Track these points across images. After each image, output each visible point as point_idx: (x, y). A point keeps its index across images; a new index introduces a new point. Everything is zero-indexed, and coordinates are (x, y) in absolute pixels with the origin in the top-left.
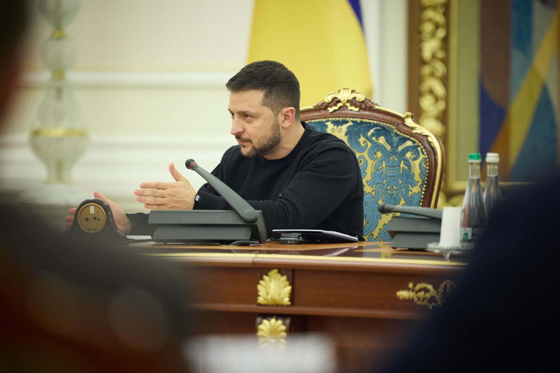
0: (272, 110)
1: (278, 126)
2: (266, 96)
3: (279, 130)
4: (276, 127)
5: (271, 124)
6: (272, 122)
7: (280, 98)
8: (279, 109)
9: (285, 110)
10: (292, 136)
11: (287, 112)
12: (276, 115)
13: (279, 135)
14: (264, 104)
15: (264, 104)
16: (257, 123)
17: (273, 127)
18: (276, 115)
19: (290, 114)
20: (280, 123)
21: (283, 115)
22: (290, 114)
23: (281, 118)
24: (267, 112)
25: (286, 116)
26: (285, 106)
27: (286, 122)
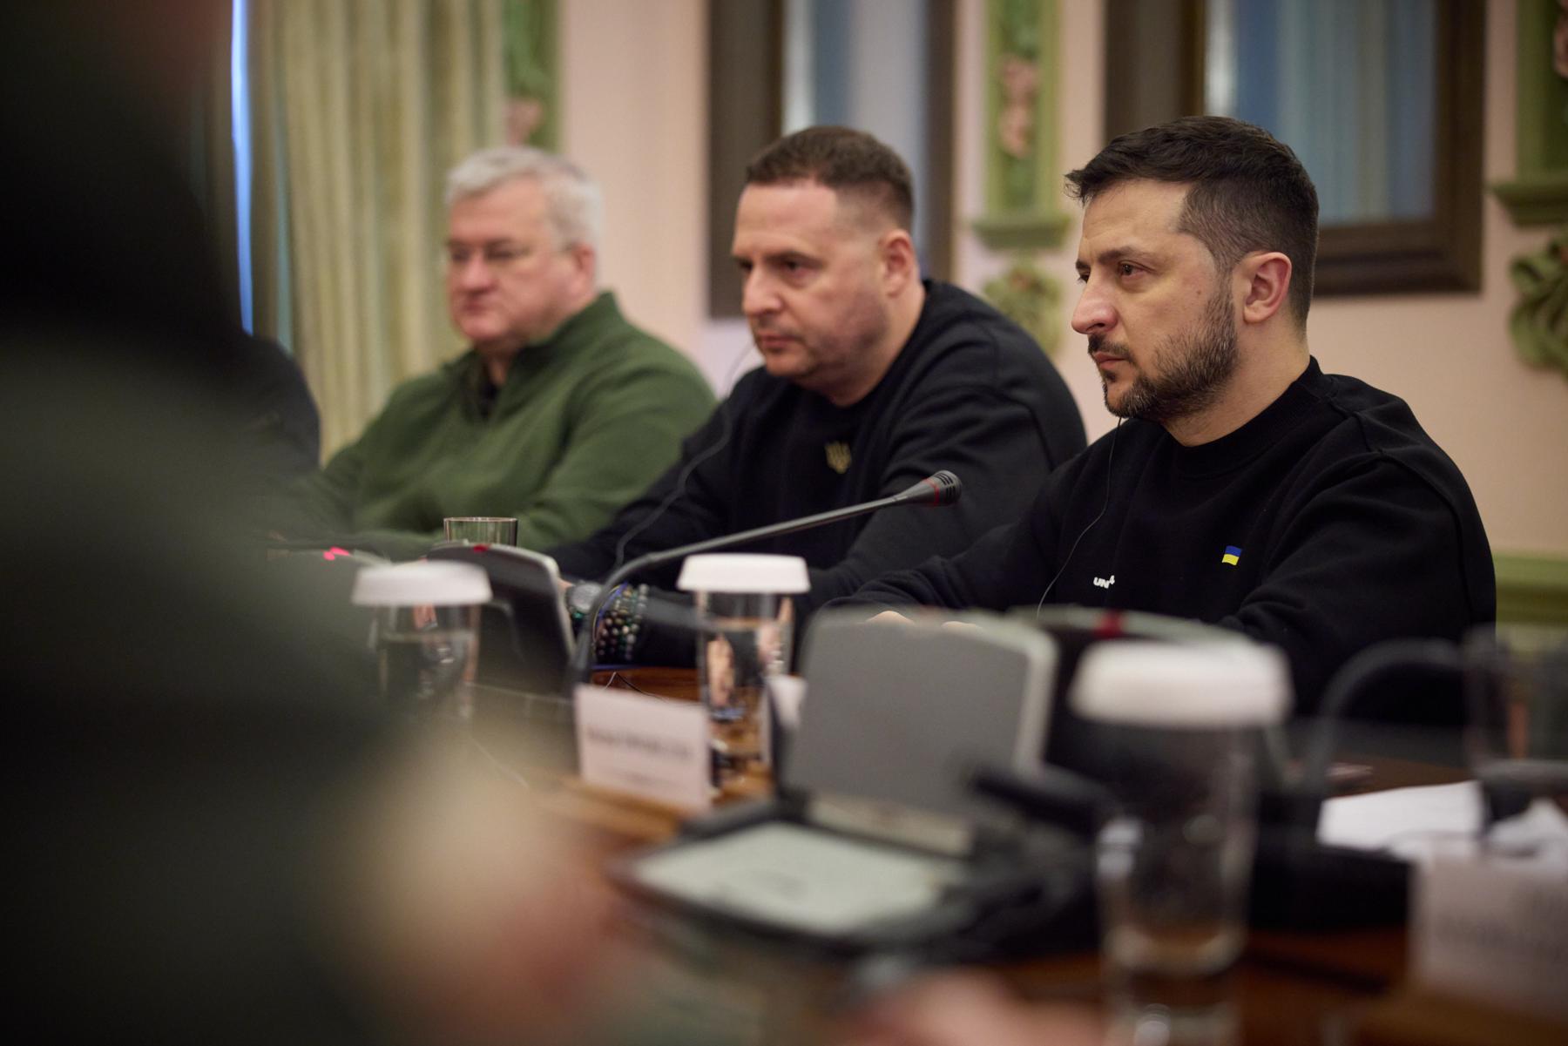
0: (1212, 251)
1: (1229, 310)
2: (1192, 201)
3: (1230, 323)
4: (1220, 312)
5: (1205, 297)
6: (1209, 288)
7: (1241, 218)
8: (1236, 250)
9: (1256, 259)
11: (1264, 266)
12: (1226, 271)
13: (1232, 342)
14: (1184, 228)
15: (1184, 228)
16: (1158, 291)
17: (1209, 308)
19: (1272, 275)
21: (1246, 275)
22: (1272, 275)
23: (1241, 287)
24: (1195, 255)
26: (1257, 246)
27: (1257, 303)
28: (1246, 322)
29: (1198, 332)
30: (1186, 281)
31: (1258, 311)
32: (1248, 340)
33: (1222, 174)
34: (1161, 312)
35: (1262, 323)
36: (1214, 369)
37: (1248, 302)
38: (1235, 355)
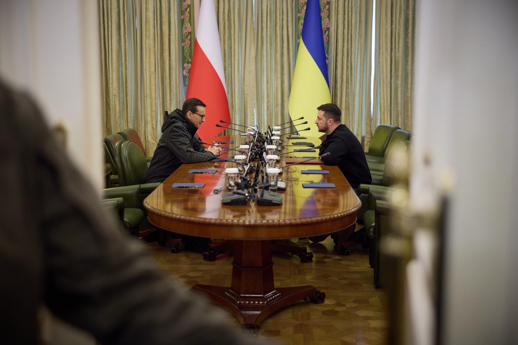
2: (325, 113)
4: (326, 124)
12: (327, 120)
16: (321, 121)
18: (327, 120)
23: (328, 122)
24: (324, 118)
31: (330, 124)
32: (329, 127)
34: (321, 123)
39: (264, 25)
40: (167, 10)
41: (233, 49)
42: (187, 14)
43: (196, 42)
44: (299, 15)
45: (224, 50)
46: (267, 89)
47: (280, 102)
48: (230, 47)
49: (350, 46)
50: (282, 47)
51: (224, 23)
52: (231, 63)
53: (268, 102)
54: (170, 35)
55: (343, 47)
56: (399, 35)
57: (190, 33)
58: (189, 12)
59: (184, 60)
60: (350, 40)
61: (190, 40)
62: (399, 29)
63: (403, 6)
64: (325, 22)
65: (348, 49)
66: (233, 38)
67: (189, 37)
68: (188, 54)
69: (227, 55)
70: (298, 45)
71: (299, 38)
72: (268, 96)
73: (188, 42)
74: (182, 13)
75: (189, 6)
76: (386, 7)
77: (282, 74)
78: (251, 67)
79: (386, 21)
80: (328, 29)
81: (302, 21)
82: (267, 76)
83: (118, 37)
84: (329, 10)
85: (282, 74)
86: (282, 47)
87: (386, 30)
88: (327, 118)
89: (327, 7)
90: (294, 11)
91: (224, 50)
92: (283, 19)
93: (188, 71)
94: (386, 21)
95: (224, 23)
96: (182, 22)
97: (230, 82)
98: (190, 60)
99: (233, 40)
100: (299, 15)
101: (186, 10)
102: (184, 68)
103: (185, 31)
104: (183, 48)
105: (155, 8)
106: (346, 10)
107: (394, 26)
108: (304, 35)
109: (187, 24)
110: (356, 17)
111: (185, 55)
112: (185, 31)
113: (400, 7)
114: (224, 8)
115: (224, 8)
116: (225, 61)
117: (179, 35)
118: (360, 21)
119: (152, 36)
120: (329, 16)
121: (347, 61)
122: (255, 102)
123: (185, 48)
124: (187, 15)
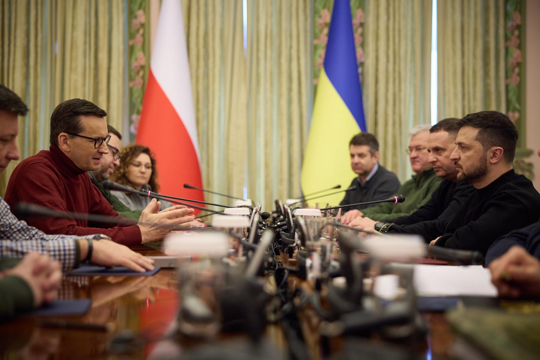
0: (483, 145)
1: (486, 160)
2: (480, 133)
3: (486, 163)
4: (484, 159)
5: (480, 156)
8: (489, 146)
9: (495, 148)
10: (498, 171)
11: (496, 150)
12: (486, 150)
13: (486, 167)
14: (477, 139)
16: (469, 153)
17: (481, 159)
18: (486, 150)
19: (498, 152)
20: (488, 158)
21: (492, 152)
22: (498, 152)
23: (490, 154)
24: (478, 146)
25: (494, 154)
27: (494, 159)
28: (491, 164)
29: (477, 164)
30: (475, 152)
31: (494, 161)
33: (488, 127)
34: (469, 158)
35: (495, 163)
36: (481, 173)
37: (492, 158)
38: (487, 170)
39: (262, 55)
40: (107, 28)
41: (210, 91)
42: (139, 37)
43: (151, 75)
44: (316, 42)
45: (198, 93)
46: (266, 155)
47: (285, 176)
48: (207, 89)
49: (397, 89)
50: (290, 90)
51: (198, 51)
52: (208, 113)
53: (267, 176)
54: (109, 68)
55: (387, 90)
56: (475, 72)
57: (142, 67)
58: (143, 35)
59: (132, 108)
60: (398, 80)
61: (143, 77)
62: (475, 65)
63: (480, 30)
64: (359, 51)
65: (394, 95)
66: (211, 73)
67: (141, 73)
68: (139, 100)
69: (201, 101)
70: (315, 90)
71: (315, 76)
72: (267, 166)
73: (139, 80)
74: (131, 35)
75: (142, 25)
76: (454, 31)
77: (290, 132)
78: (240, 119)
79: (454, 51)
80: (362, 64)
81: (321, 52)
82: (266, 133)
83: (24, 70)
84: (362, 35)
85: (290, 132)
86: (290, 90)
87: (454, 65)
88: (487, 144)
89: (360, 30)
90: (309, 34)
91: (198, 93)
92: (291, 47)
93: (137, 125)
94: (454, 51)
95: (198, 51)
96: (131, 50)
97: (205, 145)
98: (141, 108)
99: (211, 78)
100: (316, 42)
101: (138, 31)
102: (131, 122)
103: (134, 64)
104: (131, 90)
105: (87, 24)
106: (391, 34)
107: (466, 60)
108: (328, 65)
109: (138, 53)
110: (406, 45)
111: (134, 100)
112: (134, 64)
113: (476, 30)
114: (198, 28)
115: (198, 28)
116: (197, 110)
117: (124, 69)
118: (413, 52)
119: (80, 69)
120: (363, 45)
121: (394, 113)
122: (245, 176)
123: (135, 89)
124: (139, 38)
